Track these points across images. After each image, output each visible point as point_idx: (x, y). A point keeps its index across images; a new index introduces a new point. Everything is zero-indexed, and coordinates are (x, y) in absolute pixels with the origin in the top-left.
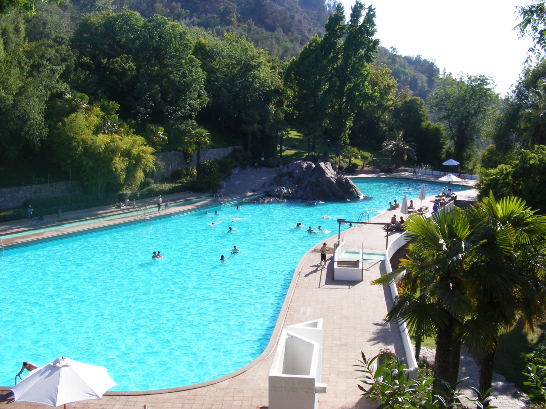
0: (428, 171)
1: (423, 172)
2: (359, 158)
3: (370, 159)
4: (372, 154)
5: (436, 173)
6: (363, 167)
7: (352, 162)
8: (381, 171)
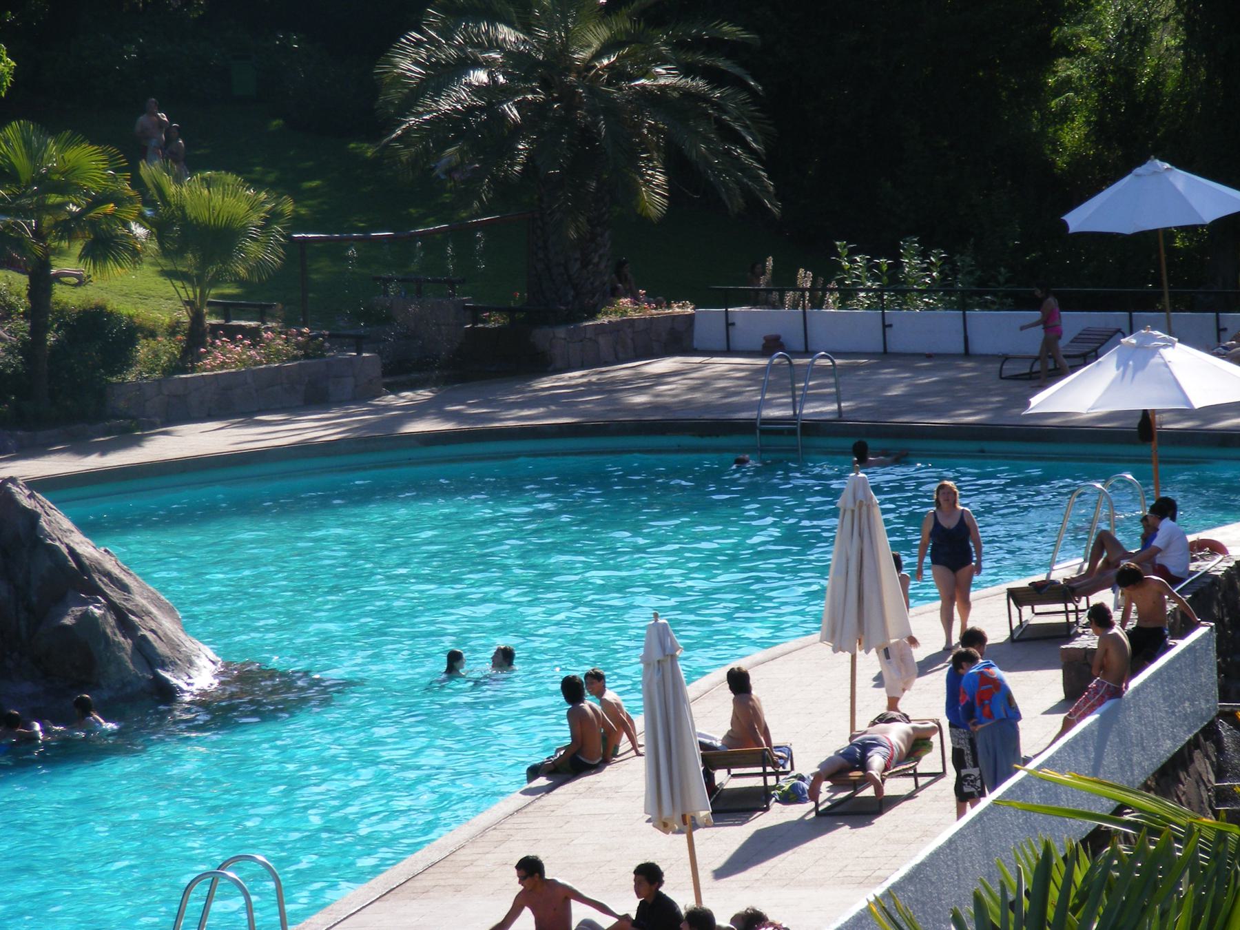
0: (927, 323)
1: (856, 335)
2: (136, 255)
3: (258, 252)
4: (280, 187)
5: (1007, 330)
6: (195, 338)
7: (65, 296)
8: (400, 374)
